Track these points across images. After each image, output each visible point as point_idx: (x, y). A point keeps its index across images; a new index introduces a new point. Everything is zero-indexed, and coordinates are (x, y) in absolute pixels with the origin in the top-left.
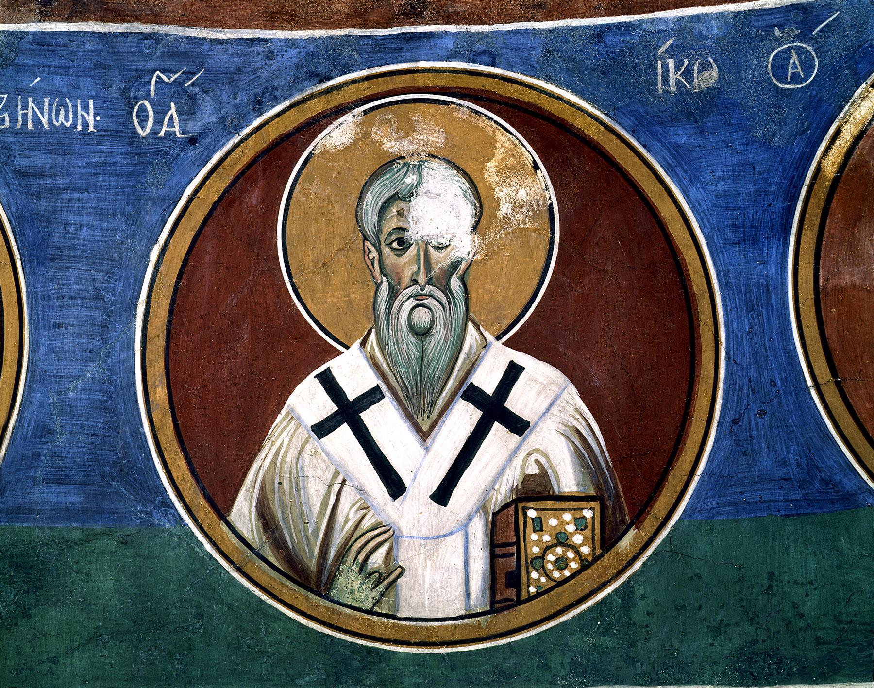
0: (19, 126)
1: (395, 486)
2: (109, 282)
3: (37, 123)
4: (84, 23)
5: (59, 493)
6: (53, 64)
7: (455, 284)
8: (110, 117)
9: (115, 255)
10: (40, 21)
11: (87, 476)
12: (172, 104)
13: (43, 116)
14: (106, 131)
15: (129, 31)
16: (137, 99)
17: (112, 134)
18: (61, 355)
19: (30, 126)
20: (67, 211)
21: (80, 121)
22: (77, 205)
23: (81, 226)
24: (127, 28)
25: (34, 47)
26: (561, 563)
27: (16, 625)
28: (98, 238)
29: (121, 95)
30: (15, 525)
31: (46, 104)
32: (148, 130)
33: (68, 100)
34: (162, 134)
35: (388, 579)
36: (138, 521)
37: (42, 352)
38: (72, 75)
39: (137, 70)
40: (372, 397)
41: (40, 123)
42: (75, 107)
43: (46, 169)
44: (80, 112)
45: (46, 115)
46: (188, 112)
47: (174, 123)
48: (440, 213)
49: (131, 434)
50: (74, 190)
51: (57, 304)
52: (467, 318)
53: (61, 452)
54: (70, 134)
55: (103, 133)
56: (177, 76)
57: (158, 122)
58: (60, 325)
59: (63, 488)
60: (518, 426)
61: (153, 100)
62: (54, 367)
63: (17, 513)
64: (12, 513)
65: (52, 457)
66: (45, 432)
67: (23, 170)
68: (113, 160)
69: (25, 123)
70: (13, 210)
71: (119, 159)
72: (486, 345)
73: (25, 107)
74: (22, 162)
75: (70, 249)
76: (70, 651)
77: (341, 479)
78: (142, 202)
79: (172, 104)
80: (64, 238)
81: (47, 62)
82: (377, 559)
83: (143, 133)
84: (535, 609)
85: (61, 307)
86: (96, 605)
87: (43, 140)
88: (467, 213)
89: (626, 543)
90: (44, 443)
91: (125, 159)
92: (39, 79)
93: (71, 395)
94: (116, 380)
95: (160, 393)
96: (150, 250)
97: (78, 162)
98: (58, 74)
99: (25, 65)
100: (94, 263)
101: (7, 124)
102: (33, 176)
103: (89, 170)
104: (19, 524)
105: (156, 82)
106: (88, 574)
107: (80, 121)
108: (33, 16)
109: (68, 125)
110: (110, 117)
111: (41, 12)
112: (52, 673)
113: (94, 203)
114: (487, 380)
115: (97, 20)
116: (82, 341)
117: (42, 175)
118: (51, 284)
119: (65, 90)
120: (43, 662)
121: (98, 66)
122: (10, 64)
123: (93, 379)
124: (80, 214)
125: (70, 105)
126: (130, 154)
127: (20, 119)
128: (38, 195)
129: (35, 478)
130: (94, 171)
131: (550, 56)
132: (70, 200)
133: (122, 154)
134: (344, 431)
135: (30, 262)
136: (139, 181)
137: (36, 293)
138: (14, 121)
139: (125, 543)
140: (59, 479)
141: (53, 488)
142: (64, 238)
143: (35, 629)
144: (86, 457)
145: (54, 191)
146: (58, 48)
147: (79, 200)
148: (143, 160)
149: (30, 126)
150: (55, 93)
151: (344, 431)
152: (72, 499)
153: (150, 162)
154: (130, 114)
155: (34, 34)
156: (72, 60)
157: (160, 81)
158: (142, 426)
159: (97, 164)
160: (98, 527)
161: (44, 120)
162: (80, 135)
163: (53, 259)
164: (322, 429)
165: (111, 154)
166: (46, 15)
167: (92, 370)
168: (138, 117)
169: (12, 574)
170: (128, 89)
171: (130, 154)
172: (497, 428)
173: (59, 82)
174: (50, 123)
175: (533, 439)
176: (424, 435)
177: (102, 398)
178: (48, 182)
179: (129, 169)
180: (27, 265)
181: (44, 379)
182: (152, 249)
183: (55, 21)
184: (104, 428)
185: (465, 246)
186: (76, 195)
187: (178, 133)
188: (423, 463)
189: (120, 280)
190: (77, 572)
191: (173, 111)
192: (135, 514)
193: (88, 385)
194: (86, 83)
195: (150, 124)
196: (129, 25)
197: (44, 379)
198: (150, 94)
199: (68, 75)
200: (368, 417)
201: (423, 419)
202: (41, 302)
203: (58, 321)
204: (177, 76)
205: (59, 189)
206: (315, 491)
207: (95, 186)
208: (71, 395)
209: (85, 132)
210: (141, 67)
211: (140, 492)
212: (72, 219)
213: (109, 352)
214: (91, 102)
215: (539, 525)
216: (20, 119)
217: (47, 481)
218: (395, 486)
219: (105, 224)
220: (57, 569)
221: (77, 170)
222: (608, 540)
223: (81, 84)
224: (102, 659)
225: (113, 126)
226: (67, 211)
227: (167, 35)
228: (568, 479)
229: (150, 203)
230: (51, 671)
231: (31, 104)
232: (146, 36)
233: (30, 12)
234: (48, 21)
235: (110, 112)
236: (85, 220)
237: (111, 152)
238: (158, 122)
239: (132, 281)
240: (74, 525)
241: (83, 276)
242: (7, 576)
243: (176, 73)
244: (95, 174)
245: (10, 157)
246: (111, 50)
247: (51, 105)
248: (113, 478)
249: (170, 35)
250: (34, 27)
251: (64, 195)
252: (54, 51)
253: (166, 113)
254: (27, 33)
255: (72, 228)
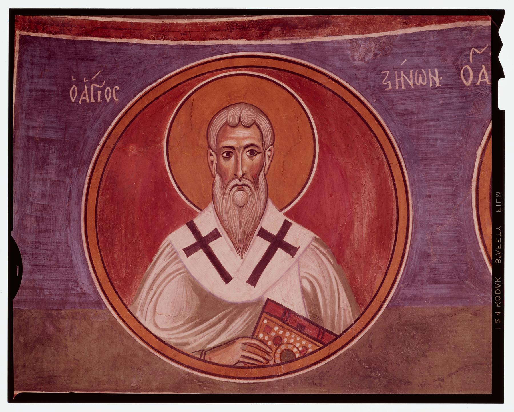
0: (397, 88)
2: (455, 170)
3: (407, 85)
4: (429, 26)
5: (436, 289)
6: (413, 51)
8: (448, 77)
9: (457, 155)
10: (404, 28)
11: (451, 278)
12: (483, 66)
13: (410, 80)
14: (446, 85)
15: (454, 27)
16: (462, 65)
17: (450, 86)
18: (431, 212)
19: (403, 87)
20: (428, 133)
21: (431, 81)
22: (433, 128)
23: (436, 140)
24: (453, 25)
25: (402, 43)
27: (419, 361)
28: (446, 146)
29: (453, 64)
30: (414, 307)
31: (411, 74)
32: (470, 82)
33: (423, 70)
34: (478, 84)
36: (482, 302)
37: (420, 212)
38: (424, 56)
39: (461, 49)
41: (409, 85)
42: (428, 73)
43: (414, 110)
44: (431, 76)
45: (412, 80)
49: (474, 254)
50: (431, 120)
51: (426, 184)
53: (436, 266)
54: (425, 89)
55: (445, 87)
56: (484, 49)
57: (476, 77)
58: (429, 196)
59: (438, 286)
61: (472, 64)
62: (428, 219)
63: (414, 300)
64: (411, 300)
65: (431, 269)
66: (426, 256)
67: (401, 112)
68: (451, 101)
69: (400, 86)
70: (398, 134)
71: (455, 100)
73: (400, 77)
74: (400, 108)
75: (431, 153)
76: (450, 375)
78: (470, 123)
79: (483, 66)
80: (427, 147)
81: (410, 50)
83: (467, 84)
85: (428, 186)
86: (462, 349)
87: (411, 94)
90: (425, 262)
91: (458, 100)
92: (406, 60)
93: (439, 234)
94: (463, 224)
96: (477, 150)
97: (432, 104)
98: (416, 56)
99: (398, 54)
100: (445, 160)
101: (390, 87)
102: (407, 115)
103: (438, 109)
104: (416, 306)
105: (473, 54)
106: (456, 332)
107: (431, 81)
108: (399, 26)
109: (424, 84)
110: (448, 77)
111: (404, 23)
112: (441, 387)
113: (442, 126)
115: (435, 23)
116: (442, 204)
117: (412, 114)
118: (422, 174)
119: (421, 65)
120: (436, 381)
121: (438, 49)
122: (389, 54)
123: (451, 225)
124: (435, 133)
125: (425, 73)
126: (461, 97)
127: (397, 83)
128: (411, 125)
129: (422, 281)
130: (440, 108)
132: (429, 126)
133: (456, 97)
135: (409, 162)
136: (468, 112)
137: (414, 179)
138: (394, 85)
139: (476, 315)
140: (436, 281)
141: (433, 286)
142: (427, 147)
143: (429, 363)
144: (450, 268)
145: (419, 122)
146: (415, 42)
147: (434, 126)
148: (469, 99)
149: (403, 87)
150: (417, 68)
152: (444, 291)
153: (473, 100)
154: (459, 74)
155: (401, 36)
156: (424, 48)
157: (475, 54)
158: (480, 249)
159: (442, 105)
160: (460, 306)
161: (411, 83)
162: (432, 89)
163: (422, 160)
165: (450, 98)
166: (407, 24)
167: (449, 220)
168: (464, 75)
169: (415, 333)
170: (457, 60)
171: (461, 97)
173: (417, 61)
174: (414, 84)
177: (456, 235)
178: (416, 117)
179: (461, 105)
180: (408, 164)
181: (422, 227)
182: (478, 149)
183: (412, 27)
184: (459, 252)
186: (432, 123)
187: (487, 82)
189: (461, 168)
190: (450, 331)
191: (484, 70)
192: (480, 298)
193: (447, 228)
194: (432, 59)
195: (471, 78)
196: (454, 24)
197: (422, 227)
198: (469, 62)
199: (422, 56)
202: (417, 184)
203: (428, 194)
204: (484, 49)
205: (423, 120)
207: (442, 117)
208: (439, 234)
209: (434, 87)
210: (463, 47)
211: (482, 286)
212: (430, 136)
213: (458, 209)
214: (436, 70)
216: (397, 83)
217: (429, 282)
219: (450, 138)
220: (439, 330)
221: (431, 109)
223: (430, 60)
224: (469, 379)
225: (450, 82)
226: (428, 133)
227: (477, 27)
229: (475, 123)
230: (440, 386)
231: (403, 75)
232: (464, 29)
233: (398, 23)
234: (408, 27)
235: (448, 74)
236: (438, 136)
237: (450, 97)
238: (476, 77)
239: (468, 168)
240: (447, 306)
241: (440, 168)
242: (412, 334)
243: (484, 47)
244: (442, 110)
245: (393, 105)
246: (445, 39)
247: (414, 74)
248: (466, 279)
249: (478, 26)
250: (400, 32)
251: (425, 124)
252: (413, 44)
253: (480, 72)
254: (397, 36)
255: (431, 142)
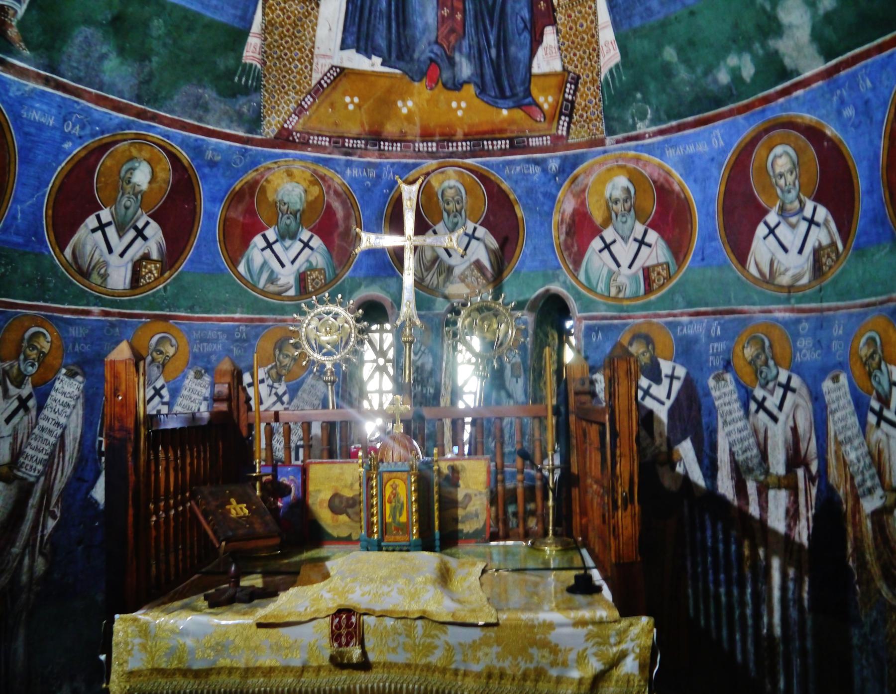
1: (110, 251)
7: (139, 197)
26: (150, 278)
35: (105, 277)
40: (109, 224)
46: (83, 127)
47: (77, 130)
48: (142, 177)
52: (140, 206)
60: (145, 239)
72: (142, 214)
77: (96, 246)
82: (103, 271)
84: (141, 290)
88: (148, 177)
89: (167, 274)
95: (50, 212)
114: (140, 225)
131: (184, 143)
134: (99, 233)
151: (99, 233)
164: (94, 231)
172: (140, 239)
175: (149, 243)
176: (120, 237)
185: (145, 186)
188: (118, 245)
200: (107, 229)
201: (121, 231)
206: (88, 248)
215: (145, 267)
218: (110, 251)
222: (162, 273)
228: (155, 256)
